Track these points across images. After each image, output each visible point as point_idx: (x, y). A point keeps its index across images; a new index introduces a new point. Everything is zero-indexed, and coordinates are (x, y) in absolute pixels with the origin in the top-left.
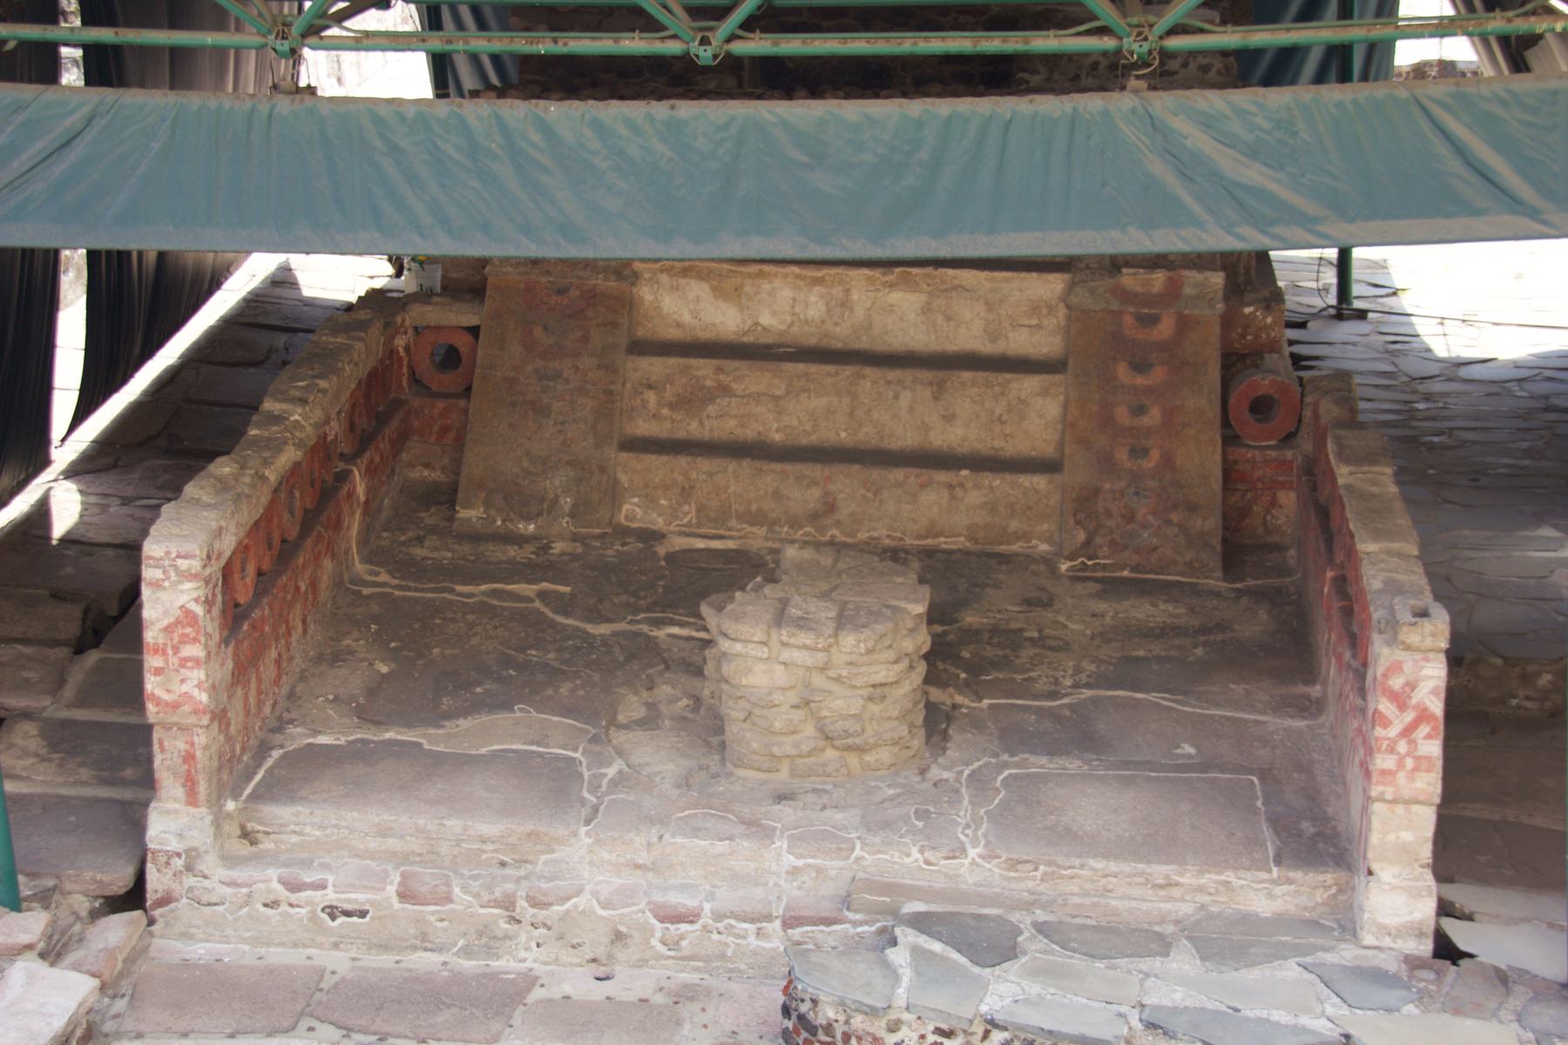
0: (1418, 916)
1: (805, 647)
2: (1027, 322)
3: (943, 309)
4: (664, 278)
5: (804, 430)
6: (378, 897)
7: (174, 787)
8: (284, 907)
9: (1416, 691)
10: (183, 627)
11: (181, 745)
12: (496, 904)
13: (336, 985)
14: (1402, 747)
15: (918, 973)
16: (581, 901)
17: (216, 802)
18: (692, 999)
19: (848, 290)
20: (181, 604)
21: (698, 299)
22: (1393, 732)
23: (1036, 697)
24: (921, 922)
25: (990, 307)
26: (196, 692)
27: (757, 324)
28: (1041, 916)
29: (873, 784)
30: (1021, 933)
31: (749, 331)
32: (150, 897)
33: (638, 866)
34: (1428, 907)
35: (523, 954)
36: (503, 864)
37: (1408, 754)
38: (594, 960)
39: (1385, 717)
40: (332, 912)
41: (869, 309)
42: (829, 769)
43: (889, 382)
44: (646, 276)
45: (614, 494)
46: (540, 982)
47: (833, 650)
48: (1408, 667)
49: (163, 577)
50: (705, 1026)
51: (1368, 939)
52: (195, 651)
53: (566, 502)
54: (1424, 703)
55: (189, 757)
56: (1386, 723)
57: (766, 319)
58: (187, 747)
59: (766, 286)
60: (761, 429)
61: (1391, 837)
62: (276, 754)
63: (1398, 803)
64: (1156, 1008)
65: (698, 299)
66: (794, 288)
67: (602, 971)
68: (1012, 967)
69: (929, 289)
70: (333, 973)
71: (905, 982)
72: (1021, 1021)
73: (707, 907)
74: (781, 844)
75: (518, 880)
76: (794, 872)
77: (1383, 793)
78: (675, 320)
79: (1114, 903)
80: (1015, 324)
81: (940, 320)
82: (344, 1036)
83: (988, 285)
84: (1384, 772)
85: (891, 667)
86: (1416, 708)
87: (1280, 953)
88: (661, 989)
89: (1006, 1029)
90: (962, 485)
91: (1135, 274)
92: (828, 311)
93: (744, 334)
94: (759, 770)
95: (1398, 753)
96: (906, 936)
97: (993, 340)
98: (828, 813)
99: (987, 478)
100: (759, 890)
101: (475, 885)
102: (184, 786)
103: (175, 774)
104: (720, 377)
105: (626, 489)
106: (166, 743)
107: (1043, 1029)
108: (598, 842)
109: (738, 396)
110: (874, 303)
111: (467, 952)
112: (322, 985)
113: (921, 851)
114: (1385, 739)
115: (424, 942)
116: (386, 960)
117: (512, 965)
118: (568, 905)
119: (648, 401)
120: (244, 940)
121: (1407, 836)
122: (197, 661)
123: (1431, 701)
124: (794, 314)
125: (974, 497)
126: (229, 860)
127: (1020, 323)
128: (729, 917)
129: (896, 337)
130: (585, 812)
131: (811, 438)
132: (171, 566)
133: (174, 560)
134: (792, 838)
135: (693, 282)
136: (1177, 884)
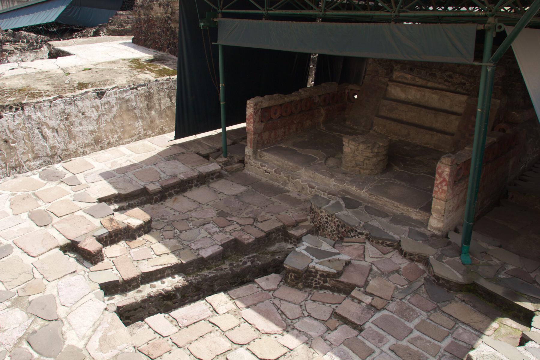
0: (439, 226)
4: (393, 86)
6: (272, 171)
14: (439, 186)
22: (438, 182)
32: (245, 162)
37: (441, 188)
40: (266, 172)
48: (442, 168)
51: (429, 229)
52: (252, 120)
56: (437, 180)
57: (409, 97)
61: (436, 207)
76: (334, 185)
84: (436, 191)
111: (282, 184)
115: (277, 181)
116: (271, 182)
121: (439, 207)
136: (399, 207)
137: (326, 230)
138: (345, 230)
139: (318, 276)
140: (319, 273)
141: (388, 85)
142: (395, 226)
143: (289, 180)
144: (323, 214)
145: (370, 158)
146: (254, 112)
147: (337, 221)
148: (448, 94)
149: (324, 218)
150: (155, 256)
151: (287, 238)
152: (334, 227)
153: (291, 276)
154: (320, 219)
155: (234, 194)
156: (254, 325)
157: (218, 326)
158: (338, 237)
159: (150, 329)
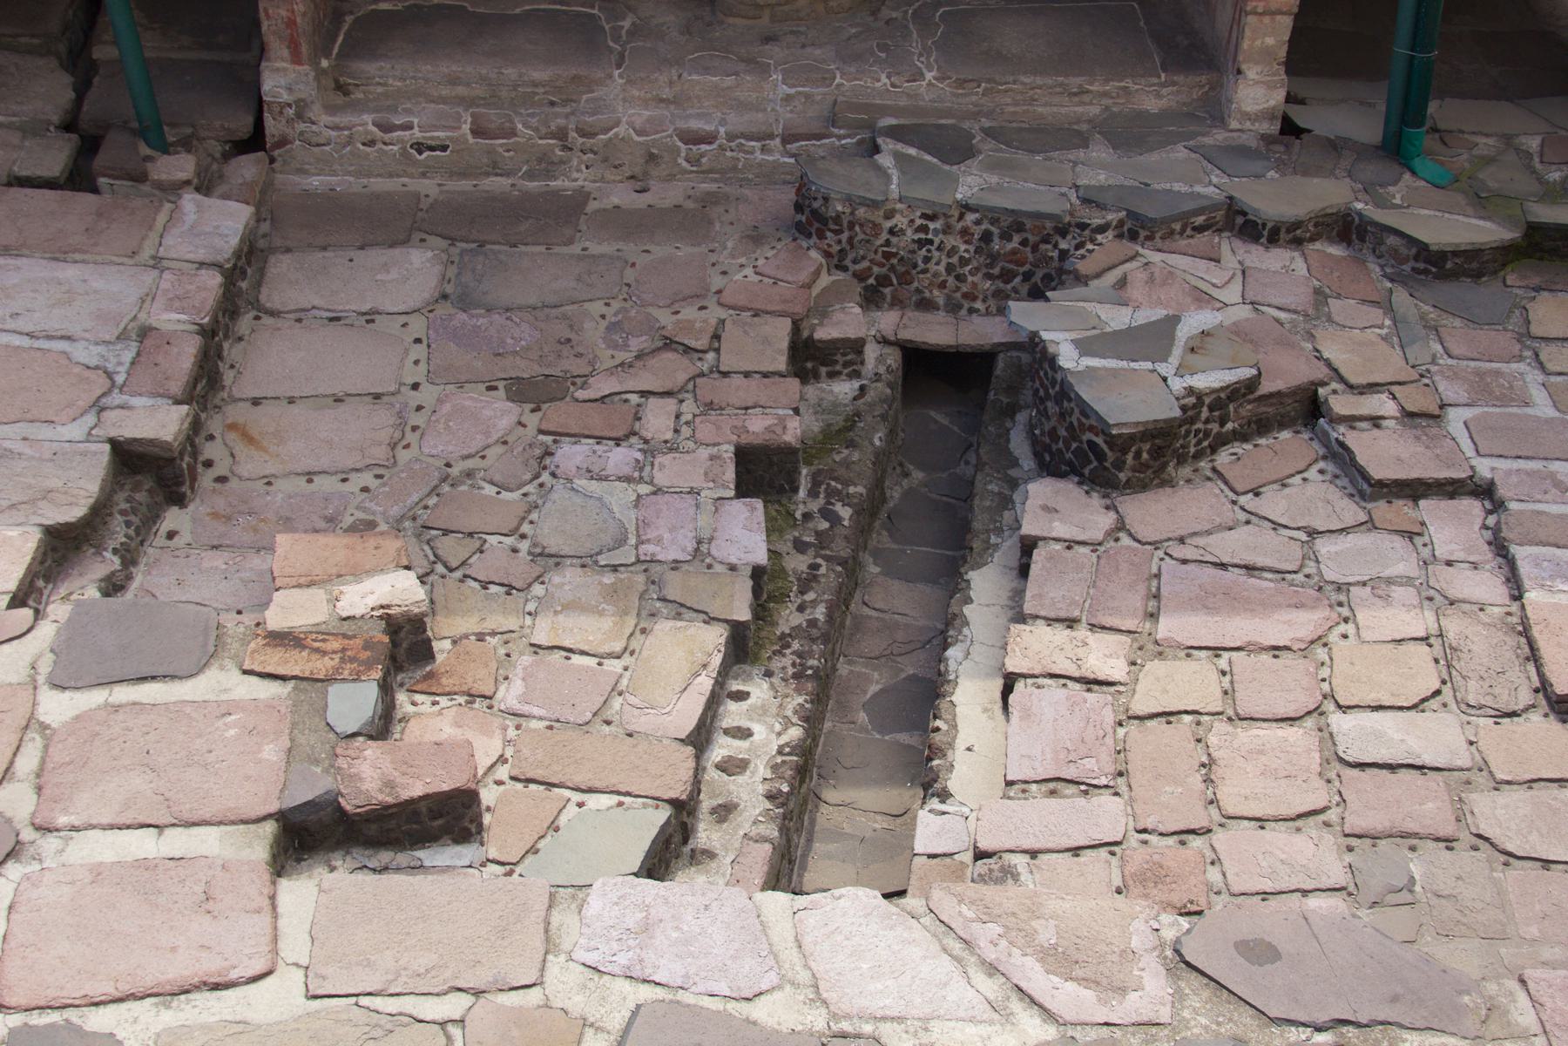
0: (1272, 103)
8: (380, 146)
11: (284, 13)
12: (553, 136)
15: (902, 172)
16: (621, 130)
17: (315, 63)
18: (716, 203)
24: (896, 133)
28: (986, 123)
30: (974, 137)
32: (269, 141)
33: (662, 100)
34: (1279, 96)
35: (575, 175)
36: (552, 104)
38: (632, 177)
40: (420, 147)
50: (732, 224)
51: (1234, 124)
55: (291, 23)
58: (289, 14)
61: (1258, 43)
62: (349, 19)
64: (1087, 187)
67: (639, 186)
68: (973, 164)
70: (427, 196)
71: (895, 179)
73: (722, 130)
74: (777, 76)
75: (567, 116)
76: (788, 99)
77: (1256, 7)
79: (1040, 109)
87: (1169, 140)
88: (689, 197)
96: (887, 144)
98: (809, 50)
100: (760, 115)
101: (534, 121)
102: (289, 47)
103: (280, 38)
108: (629, 82)
111: (530, 176)
112: (421, 206)
113: (889, 77)
115: (496, 169)
116: (465, 185)
117: (567, 183)
118: (611, 134)
120: (349, 173)
121: (1270, 41)
126: (331, 109)
130: (614, 58)
134: (784, 72)
136: (1088, 91)
137: (925, 271)
138: (1024, 243)
139: (1205, 413)
140: (1207, 401)
143: (566, 148)
144: (900, 221)
147: (978, 222)
149: (909, 232)
150: (614, 666)
151: (809, 365)
152: (963, 247)
153: (1138, 455)
154: (888, 243)
155: (426, 295)
156: (1249, 643)
157: (1186, 712)
158: (988, 276)
159: (1043, 857)
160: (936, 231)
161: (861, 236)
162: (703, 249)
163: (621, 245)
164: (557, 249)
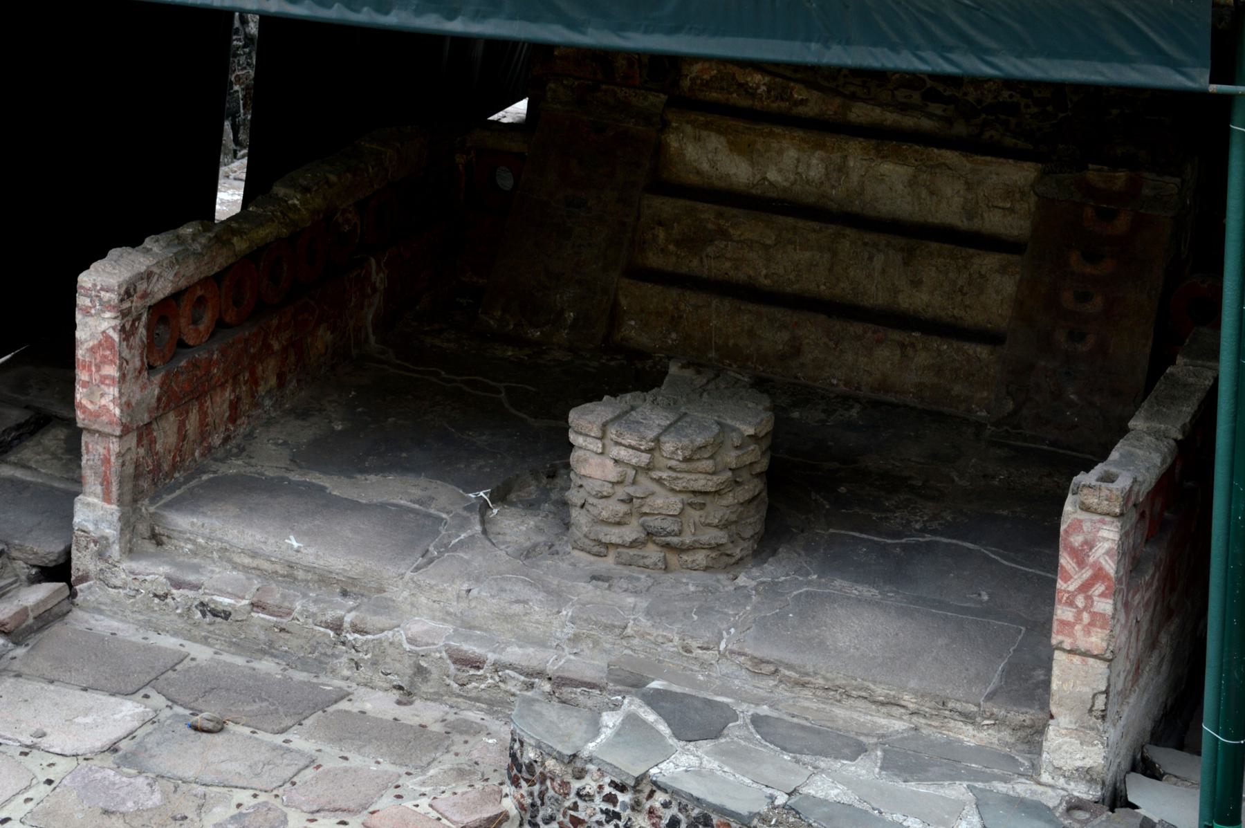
0: (1089, 763)
1: (630, 447)
2: (1001, 205)
3: (928, 183)
5: (789, 279)
7: (95, 484)
9: (1093, 551)
10: (104, 350)
13: (188, 670)
14: (1080, 601)
19: (846, 156)
20: (103, 329)
21: (716, 151)
22: (1072, 586)
23: (879, 534)
25: (969, 186)
26: (111, 406)
27: (765, 179)
28: (764, 710)
29: (684, 580)
31: (757, 184)
37: (1085, 608)
39: (1066, 571)
41: (862, 176)
42: (648, 562)
43: (865, 244)
44: (674, 125)
45: (615, 316)
46: (351, 697)
47: (657, 454)
48: (1087, 526)
49: (90, 304)
51: (1046, 777)
52: (111, 371)
53: (569, 316)
54: (1100, 563)
55: (106, 461)
56: (1067, 578)
57: (773, 175)
58: (105, 452)
59: (775, 145)
60: (751, 273)
63: (1075, 654)
64: (807, 796)
65: (716, 151)
66: (799, 150)
69: (916, 163)
70: (193, 659)
72: (678, 786)
77: (1061, 642)
78: (696, 168)
80: (990, 204)
81: (924, 193)
82: (167, 706)
83: (969, 165)
84: (1063, 623)
85: (709, 477)
86: (1093, 566)
89: (665, 791)
90: (913, 345)
91: (1099, 170)
92: (827, 175)
93: (754, 186)
94: (589, 552)
95: (1077, 607)
96: (633, 705)
97: (970, 217)
99: (936, 342)
102: (102, 484)
103: (95, 473)
104: (720, 221)
105: (625, 311)
106: (90, 446)
107: (692, 795)
109: (734, 241)
110: (867, 171)
114: (1065, 591)
115: (268, 650)
119: (658, 236)
122: (113, 378)
123: (1106, 561)
124: (797, 173)
125: (922, 358)
127: (995, 204)
128: (508, 669)
129: (885, 204)
131: (794, 287)
132: (97, 296)
133: (98, 292)
135: (713, 135)
141: (665, 125)
142: (912, 786)
144: (589, 784)
145: (708, 499)
146: (123, 330)
147: (666, 805)
148: (951, 156)
149: (598, 799)
154: (575, 807)
155: (98, 744)
160: (624, 805)
161: (551, 793)
162: (403, 770)
163: (327, 748)
164: (261, 735)
